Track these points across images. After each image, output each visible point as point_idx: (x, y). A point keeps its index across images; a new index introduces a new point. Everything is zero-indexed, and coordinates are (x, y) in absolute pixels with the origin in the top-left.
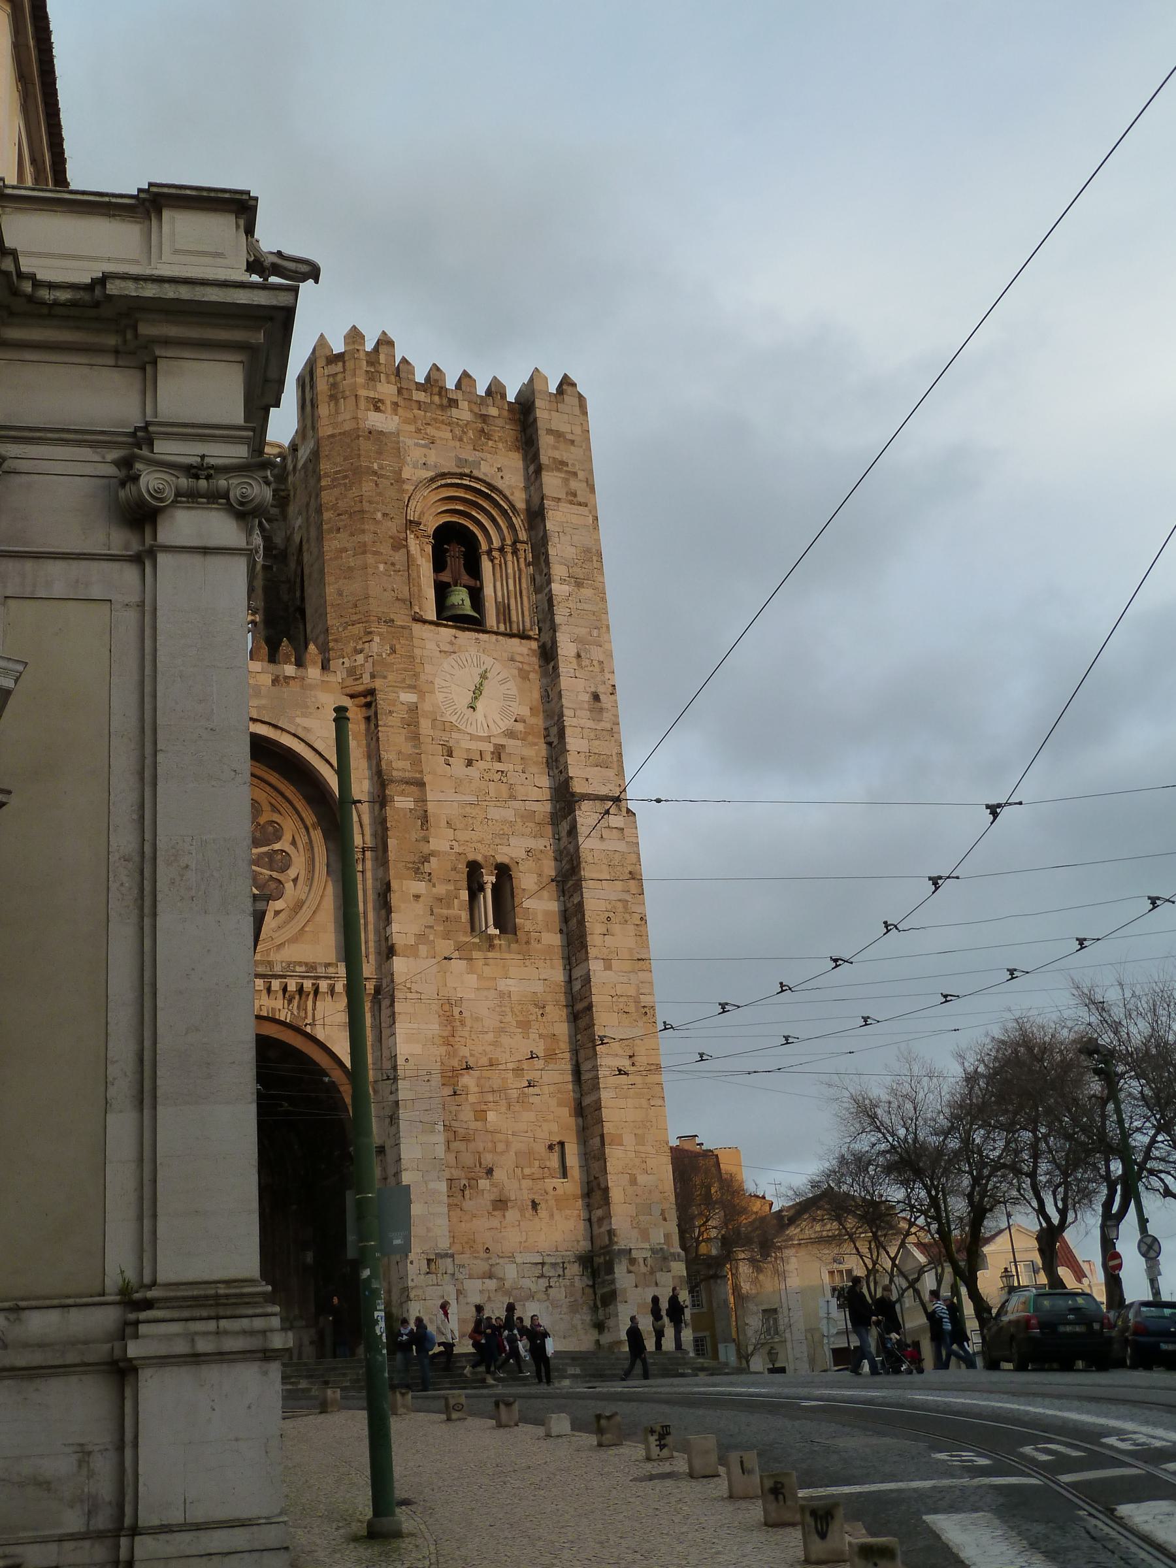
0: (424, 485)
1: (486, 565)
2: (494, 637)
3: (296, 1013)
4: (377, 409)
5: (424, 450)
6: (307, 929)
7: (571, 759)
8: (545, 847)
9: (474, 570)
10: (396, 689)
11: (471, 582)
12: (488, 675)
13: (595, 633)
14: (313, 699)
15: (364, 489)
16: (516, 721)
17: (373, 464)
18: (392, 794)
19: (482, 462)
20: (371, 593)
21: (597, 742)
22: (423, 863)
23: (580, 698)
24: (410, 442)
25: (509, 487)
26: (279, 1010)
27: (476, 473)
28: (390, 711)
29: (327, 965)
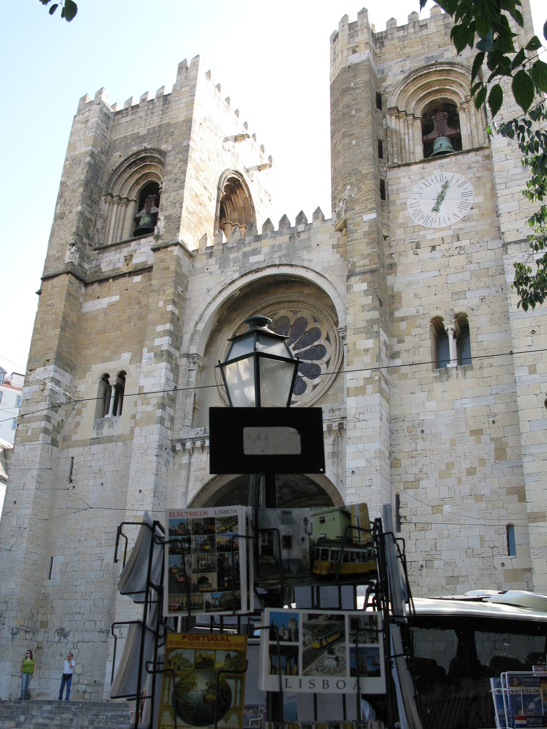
0: (402, 82)
1: (462, 116)
4: (354, 52)
5: (401, 63)
6: (329, 393)
7: (502, 219)
8: (497, 292)
10: (361, 214)
12: (450, 184)
15: (344, 101)
16: (472, 208)
17: (350, 84)
18: (351, 284)
19: (445, 52)
22: (372, 327)
23: (510, 173)
24: (391, 63)
25: (466, 58)
27: (439, 61)
28: (356, 230)
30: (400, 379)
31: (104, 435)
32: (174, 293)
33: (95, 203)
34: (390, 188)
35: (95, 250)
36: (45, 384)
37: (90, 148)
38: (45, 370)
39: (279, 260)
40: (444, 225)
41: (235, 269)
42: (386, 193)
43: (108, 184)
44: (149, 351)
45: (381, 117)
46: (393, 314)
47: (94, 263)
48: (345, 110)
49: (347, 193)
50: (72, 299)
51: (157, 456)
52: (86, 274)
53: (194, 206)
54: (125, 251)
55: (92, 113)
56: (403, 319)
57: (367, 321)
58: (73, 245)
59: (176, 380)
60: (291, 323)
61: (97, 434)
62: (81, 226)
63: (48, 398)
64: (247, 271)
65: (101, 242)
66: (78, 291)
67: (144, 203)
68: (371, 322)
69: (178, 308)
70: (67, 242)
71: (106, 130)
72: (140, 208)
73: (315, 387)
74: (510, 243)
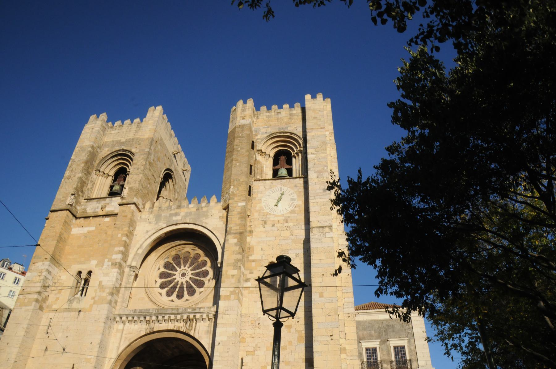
1: (294, 160)
2: (288, 180)
3: (188, 328)
4: (243, 119)
5: (266, 129)
6: (208, 297)
9: (290, 162)
11: (288, 167)
12: (285, 193)
13: (325, 168)
14: (211, 213)
15: (235, 142)
16: (295, 207)
20: (232, 173)
21: (324, 206)
22: (237, 263)
25: (299, 132)
26: (182, 327)
27: (285, 131)
29: (200, 308)
30: (249, 293)
31: (73, 307)
32: (128, 230)
33: (89, 174)
34: (253, 191)
35: (85, 199)
36: (42, 272)
37: (92, 143)
38: (43, 264)
39: (189, 221)
40: (280, 214)
41: (164, 222)
42: (251, 193)
43: (98, 164)
44: (109, 261)
45: (253, 153)
46: (248, 257)
47: (83, 207)
48: (235, 147)
49: (231, 190)
50: (66, 225)
51: (105, 323)
52: (77, 212)
53: (146, 184)
54: (103, 203)
55: (96, 125)
56: (253, 261)
57: (235, 260)
58: (72, 195)
59: (122, 281)
60: (191, 256)
61: (69, 306)
62: (79, 185)
63: (42, 281)
64: (171, 224)
65: (89, 196)
66: (71, 221)
67: (117, 178)
68: (238, 261)
69: (129, 239)
70: (69, 193)
71: (102, 135)
72: (114, 181)
73: (200, 293)
74: (315, 227)
